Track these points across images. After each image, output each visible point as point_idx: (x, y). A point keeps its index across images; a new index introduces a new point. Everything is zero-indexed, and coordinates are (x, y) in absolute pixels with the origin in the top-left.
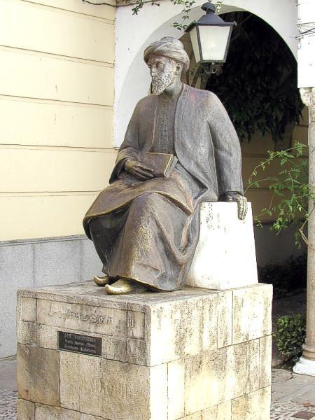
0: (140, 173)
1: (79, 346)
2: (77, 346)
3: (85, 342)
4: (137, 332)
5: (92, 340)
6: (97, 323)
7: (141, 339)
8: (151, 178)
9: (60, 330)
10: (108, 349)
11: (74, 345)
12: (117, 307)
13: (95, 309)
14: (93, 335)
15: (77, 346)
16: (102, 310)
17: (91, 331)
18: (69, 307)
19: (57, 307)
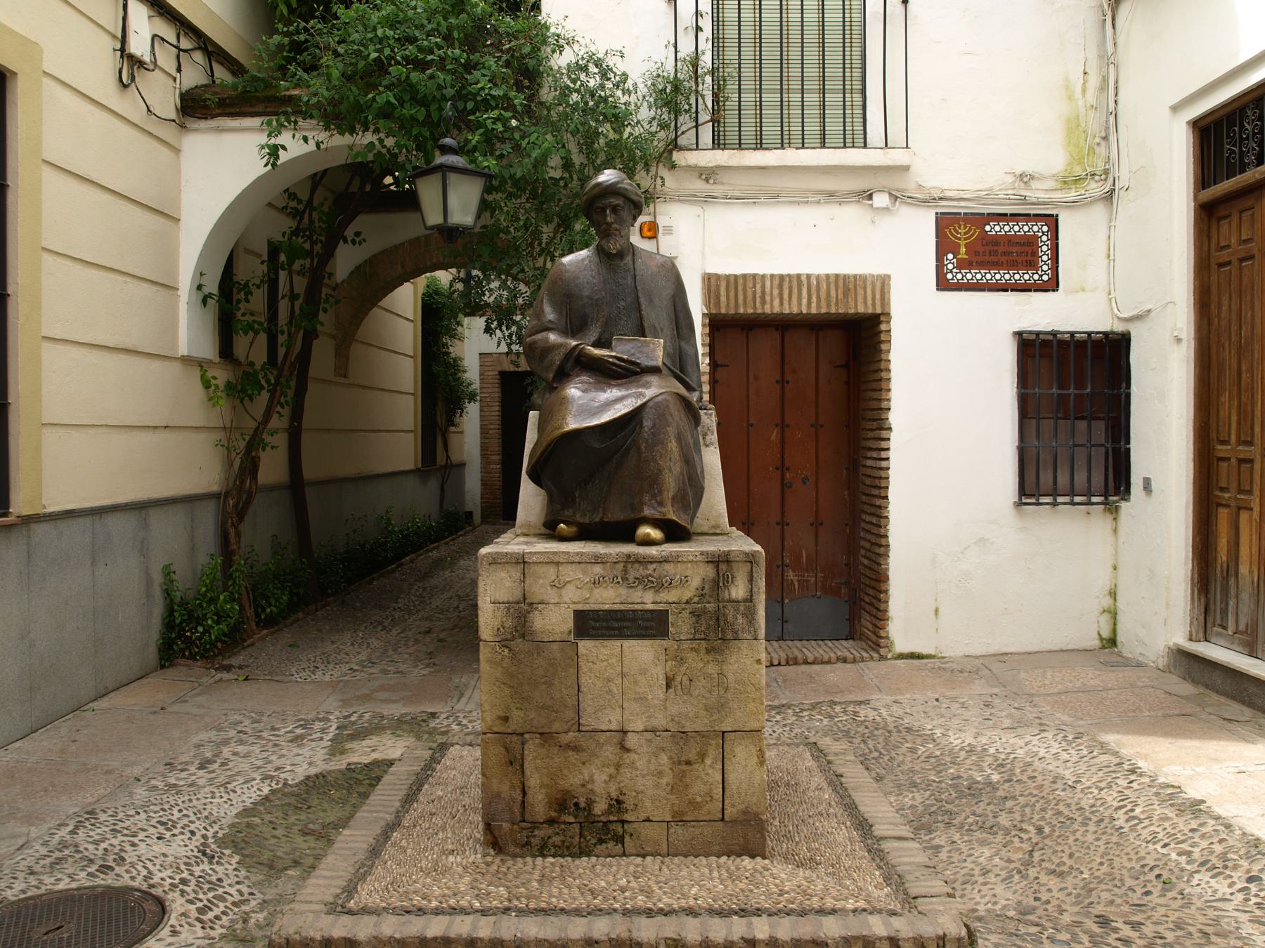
0: (619, 366)
1: (619, 629)
2: (614, 629)
3: (634, 620)
4: (738, 591)
5: (649, 615)
6: (660, 585)
7: (745, 601)
8: (636, 374)
9: (579, 607)
10: (681, 625)
11: (607, 628)
12: (699, 558)
13: (654, 566)
14: (650, 607)
15: (614, 629)
16: (667, 567)
17: (647, 600)
18: (598, 569)
19: (569, 573)
